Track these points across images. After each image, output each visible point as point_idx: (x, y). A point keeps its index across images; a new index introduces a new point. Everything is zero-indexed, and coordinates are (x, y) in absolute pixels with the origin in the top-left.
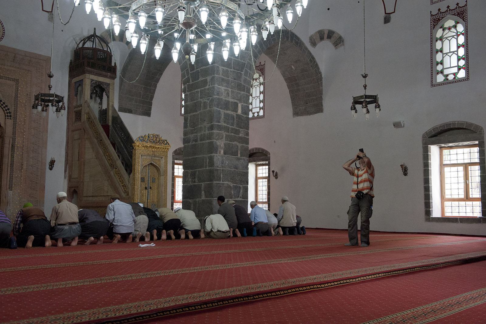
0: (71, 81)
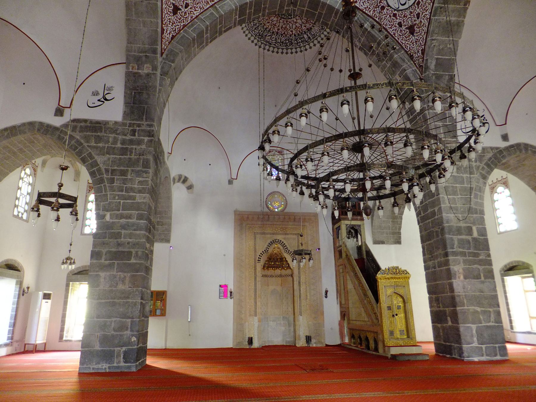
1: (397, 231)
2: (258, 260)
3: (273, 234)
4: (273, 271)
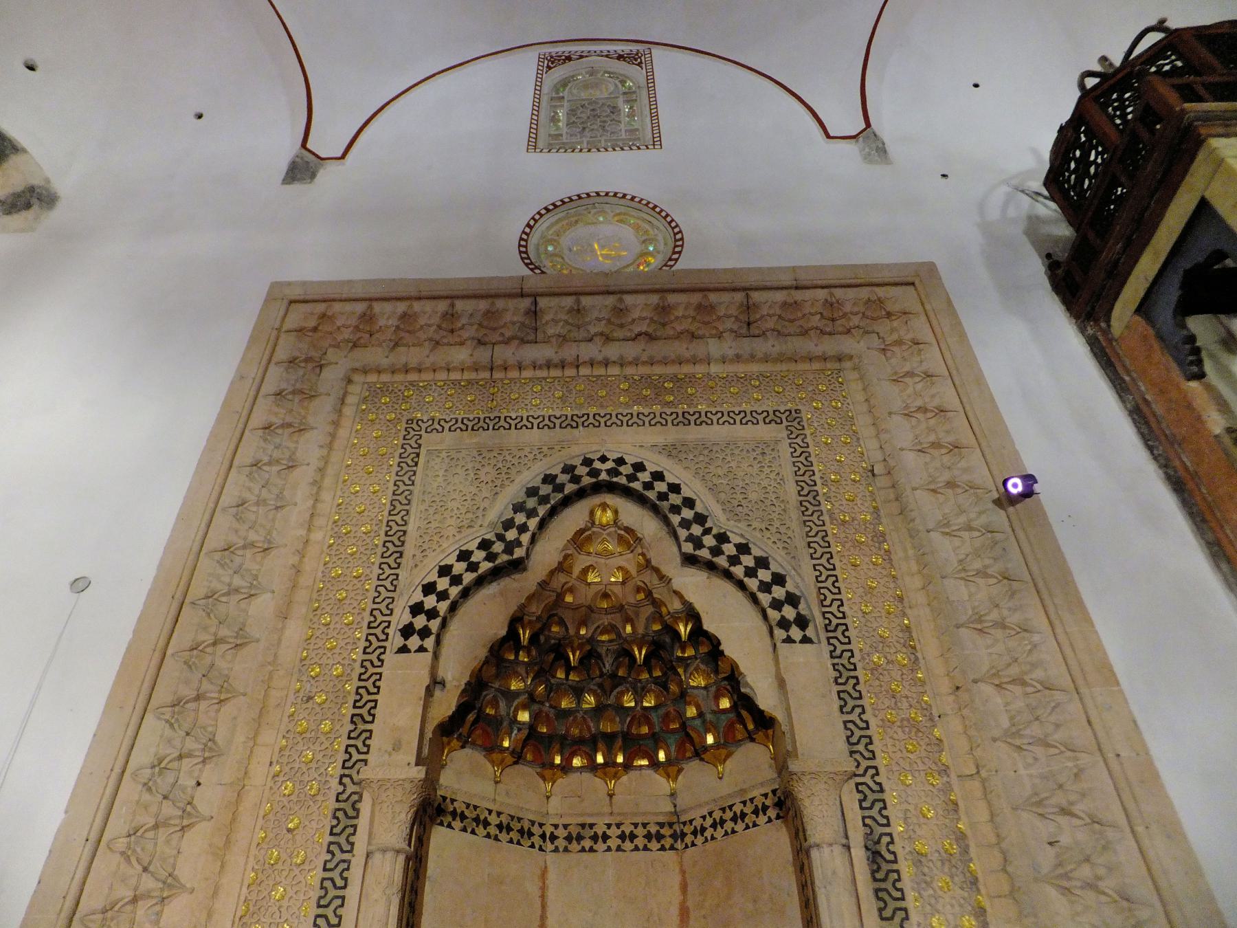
0: (1107, 332)
2: (407, 631)
3: (572, 423)
4: (597, 784)
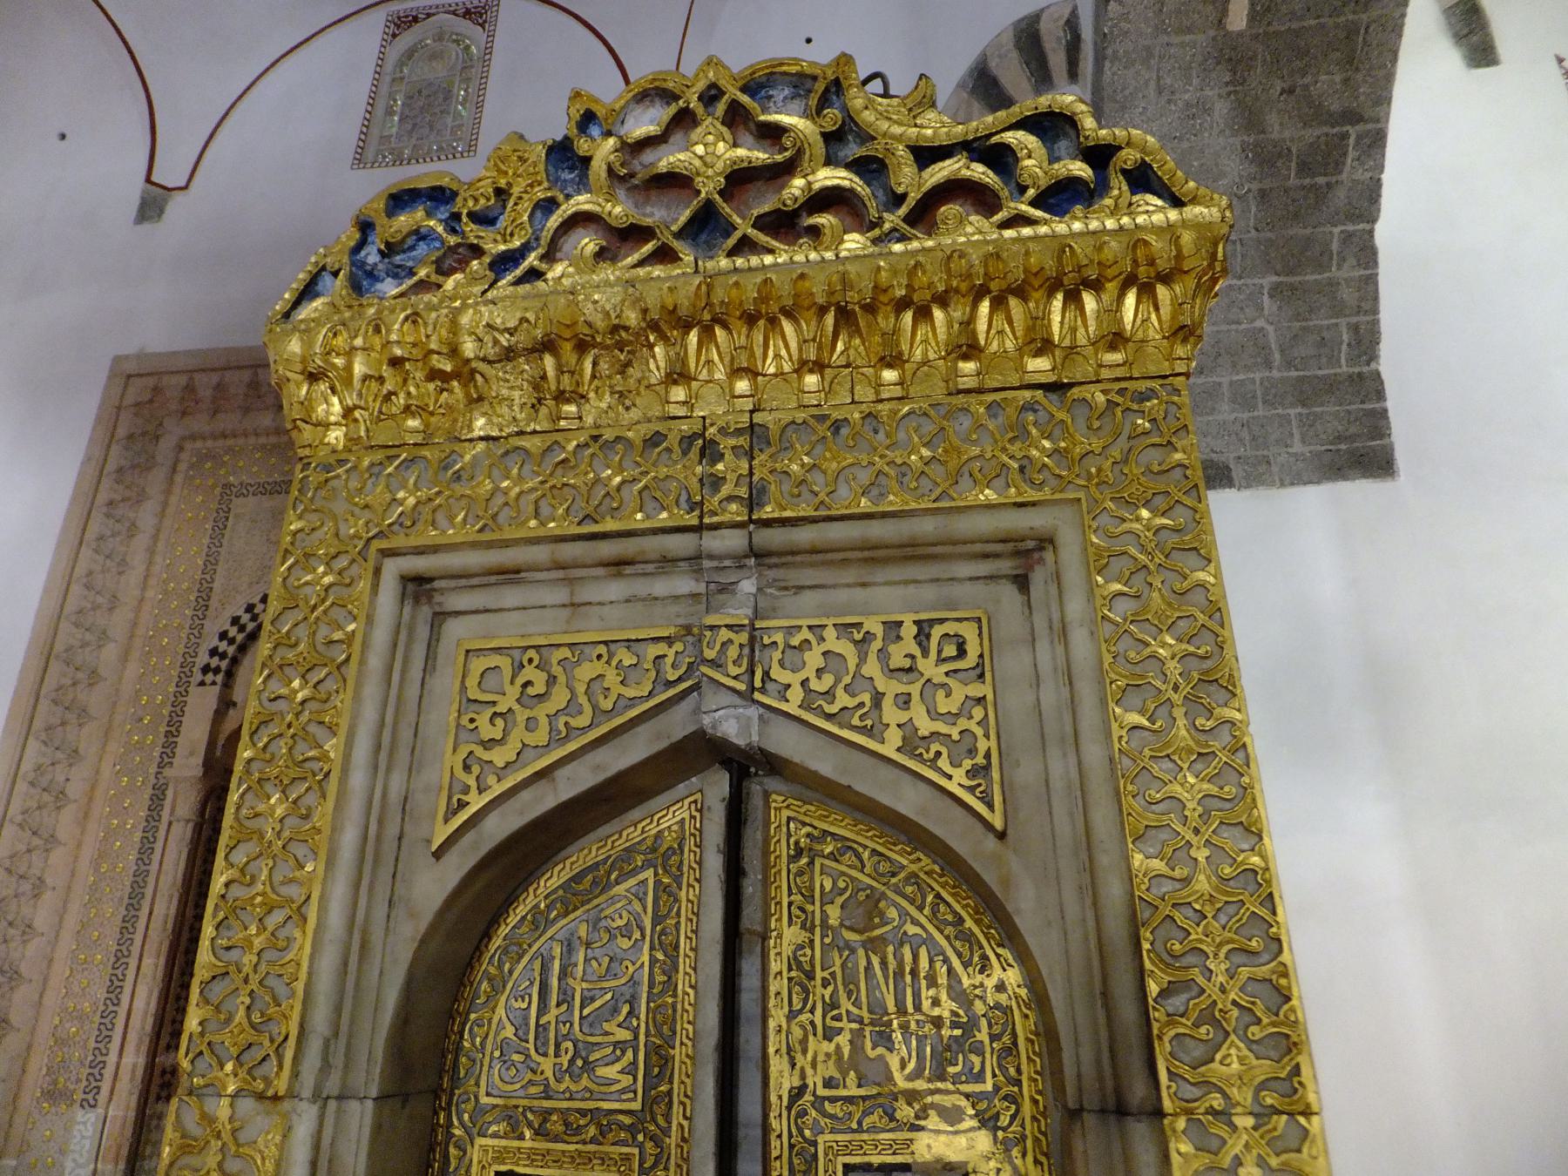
1: (1345, 369)
